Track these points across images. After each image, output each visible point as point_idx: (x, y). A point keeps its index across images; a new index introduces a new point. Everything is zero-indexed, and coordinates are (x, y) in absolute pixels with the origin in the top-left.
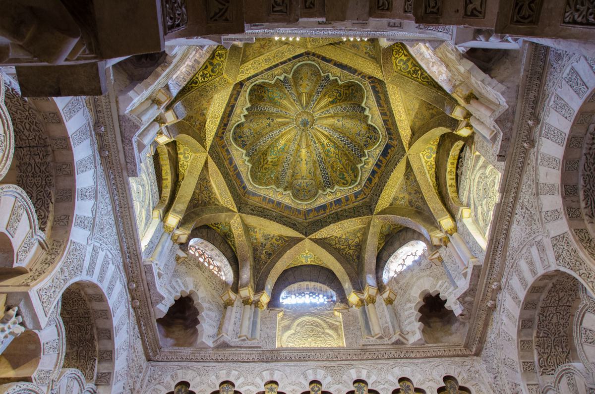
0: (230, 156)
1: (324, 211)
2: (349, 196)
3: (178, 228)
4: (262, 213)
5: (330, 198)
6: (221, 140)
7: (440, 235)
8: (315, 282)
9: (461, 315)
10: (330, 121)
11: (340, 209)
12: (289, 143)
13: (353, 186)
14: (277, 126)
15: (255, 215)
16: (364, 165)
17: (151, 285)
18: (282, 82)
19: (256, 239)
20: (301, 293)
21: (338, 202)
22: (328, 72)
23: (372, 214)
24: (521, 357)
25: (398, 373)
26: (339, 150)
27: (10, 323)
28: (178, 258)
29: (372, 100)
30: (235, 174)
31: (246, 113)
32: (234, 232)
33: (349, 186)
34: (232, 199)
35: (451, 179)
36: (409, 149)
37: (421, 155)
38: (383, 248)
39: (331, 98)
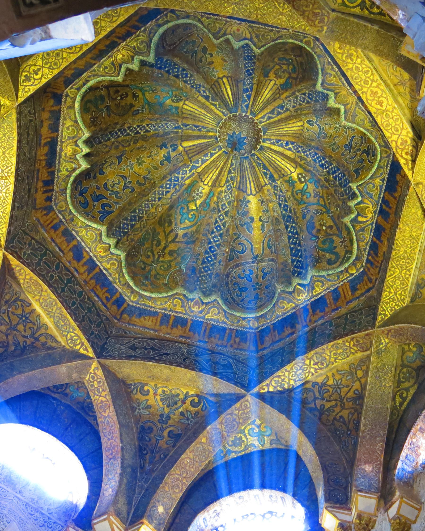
0: (74, 242)
1: (292, 328)
2: (341, 290)
6: (46, 215)
11: (322, 321)
12: (219, 189)
13: (346, 265)
14: (186, 157)
15: (135, 358)
16: (356, 217)
18: (160, 68)
19: (149, 407)
22: (225, 34)
23: (373, 327)
26: (322, 187)
29: (333, 73)
30: (91, 279)
31: (86, 150)
32: (93, 399)
33: (340, 265)
34: (78, 331)
36: (413, 173)
39: (280, 77)
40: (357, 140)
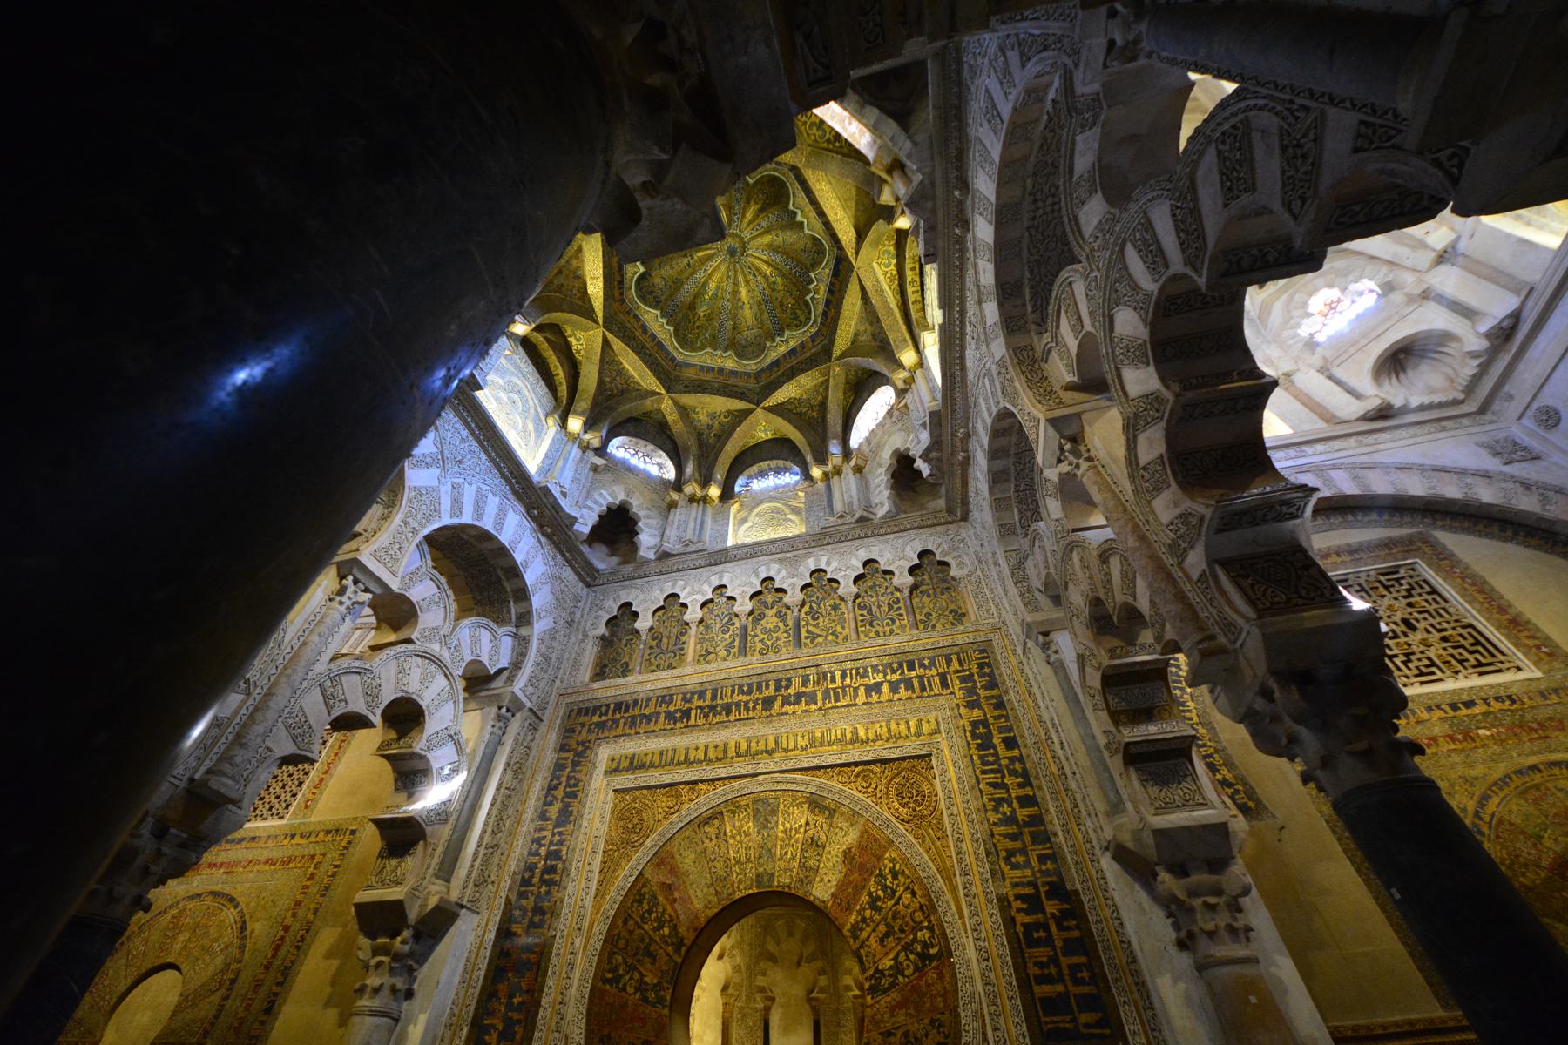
3: (585, 432)
4: (701, 387)
5: (783, 349)
7: (903, 375)
8: (778, 458)
9: (930, 475)
10: (767, 239)
17: (556, 506)
20: (763, 474)
21: (793, 352)
24: (998, 519)
25: (864, 555)
27: (349, 592)
28: (595, 469)
35: (914, 293)
37: (875, 265)
38: (853, 403)
40: (809, 244)
